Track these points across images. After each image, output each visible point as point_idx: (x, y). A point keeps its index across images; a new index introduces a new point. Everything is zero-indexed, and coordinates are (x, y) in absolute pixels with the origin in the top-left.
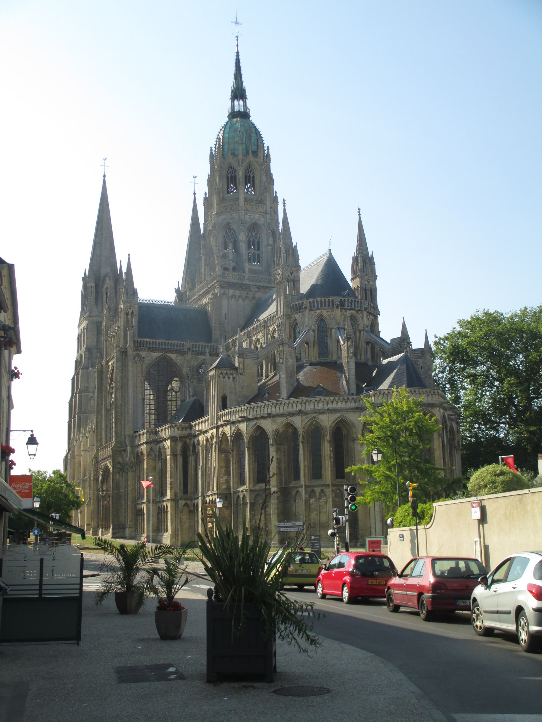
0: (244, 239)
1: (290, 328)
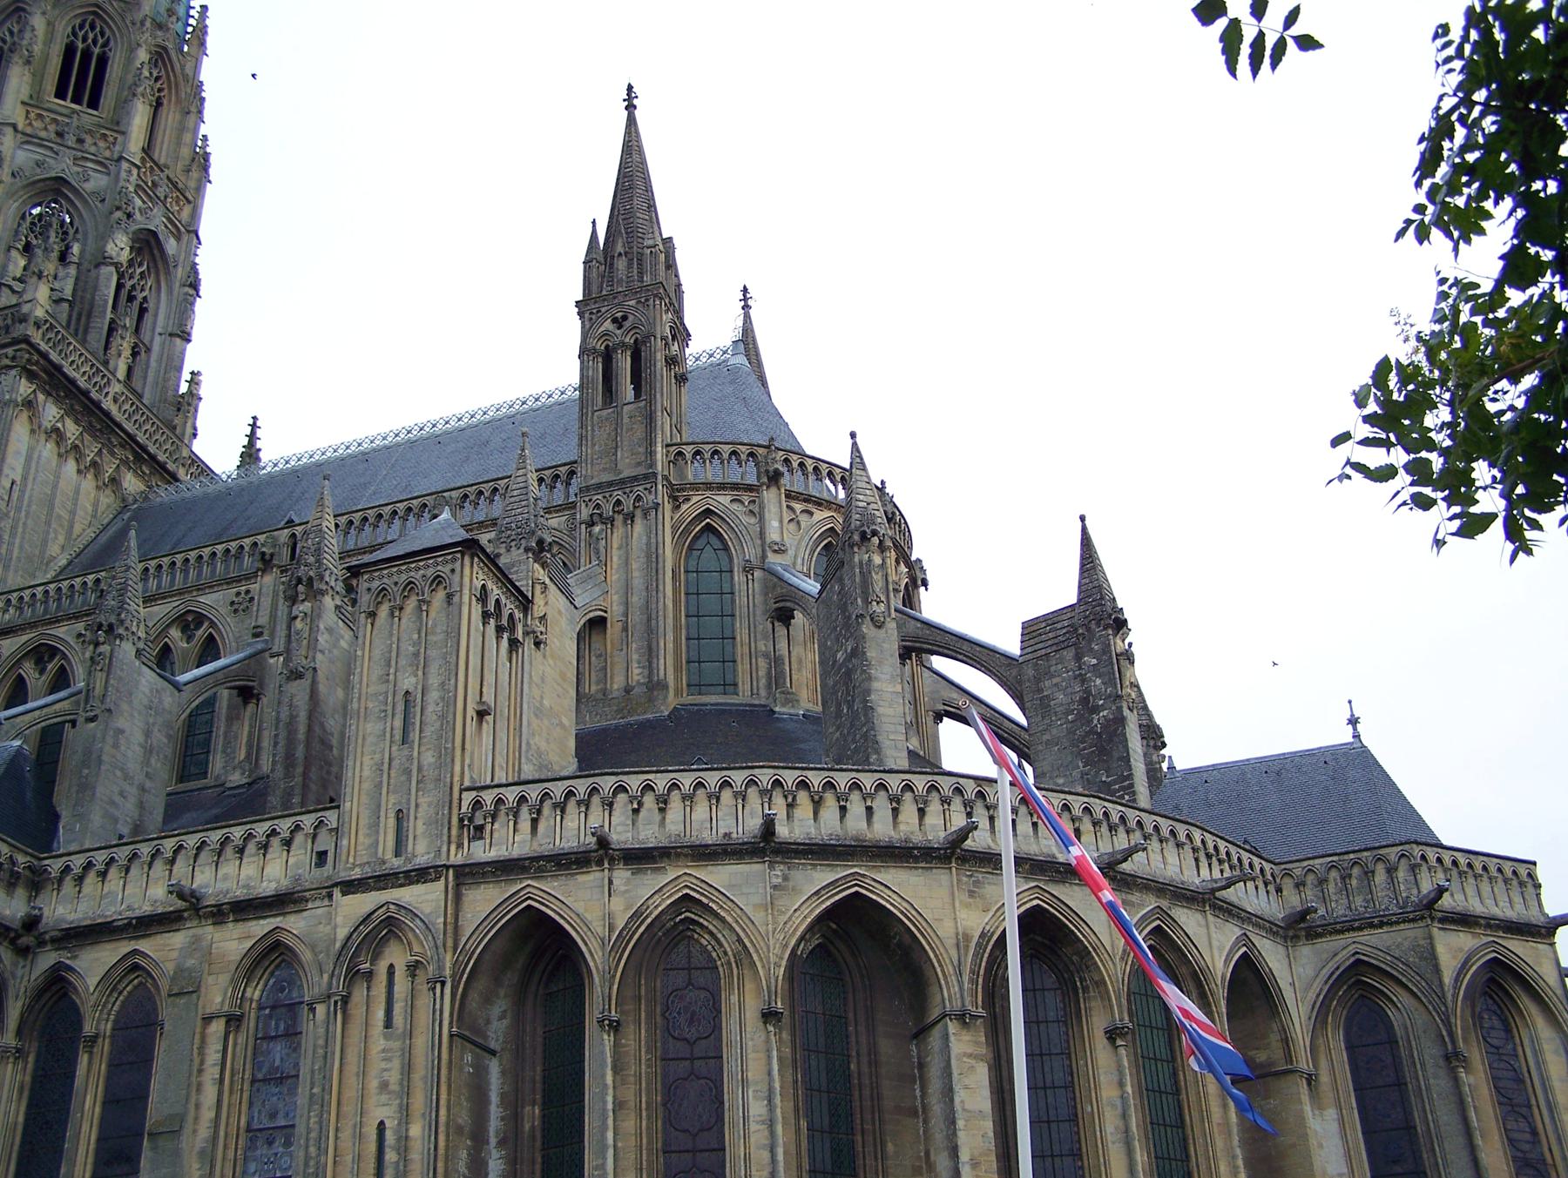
0: (125, 256)
1: (677, 546)
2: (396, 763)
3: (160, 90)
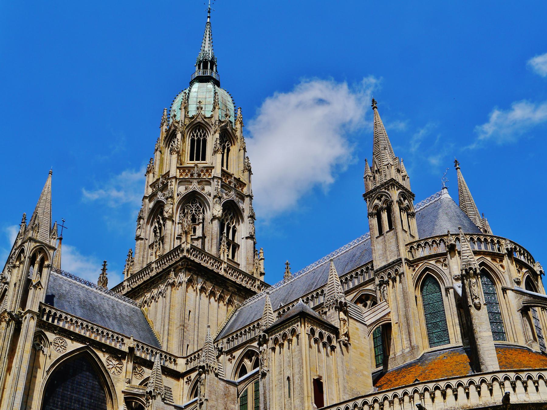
2: (287, 407)
3: (228, 145)
